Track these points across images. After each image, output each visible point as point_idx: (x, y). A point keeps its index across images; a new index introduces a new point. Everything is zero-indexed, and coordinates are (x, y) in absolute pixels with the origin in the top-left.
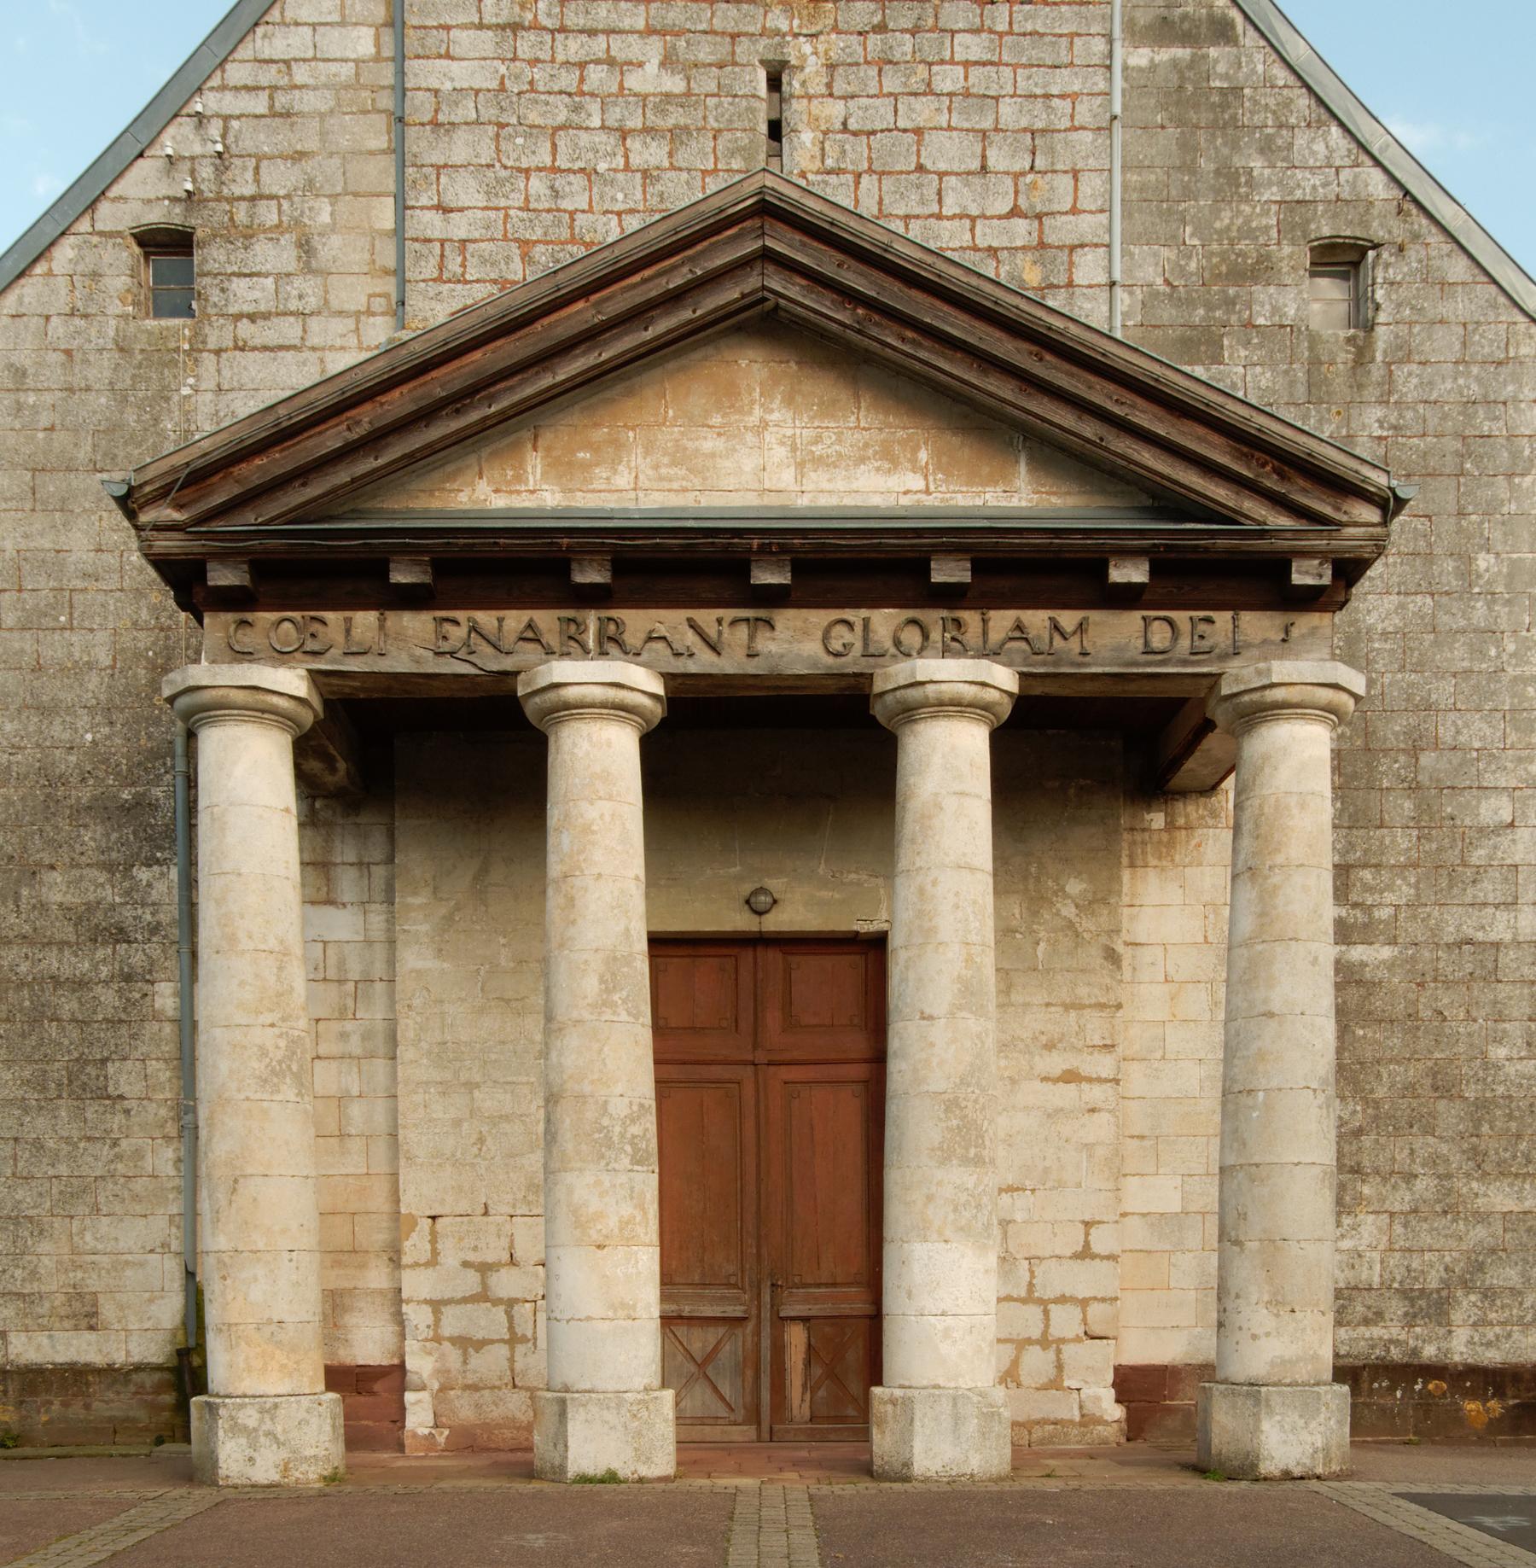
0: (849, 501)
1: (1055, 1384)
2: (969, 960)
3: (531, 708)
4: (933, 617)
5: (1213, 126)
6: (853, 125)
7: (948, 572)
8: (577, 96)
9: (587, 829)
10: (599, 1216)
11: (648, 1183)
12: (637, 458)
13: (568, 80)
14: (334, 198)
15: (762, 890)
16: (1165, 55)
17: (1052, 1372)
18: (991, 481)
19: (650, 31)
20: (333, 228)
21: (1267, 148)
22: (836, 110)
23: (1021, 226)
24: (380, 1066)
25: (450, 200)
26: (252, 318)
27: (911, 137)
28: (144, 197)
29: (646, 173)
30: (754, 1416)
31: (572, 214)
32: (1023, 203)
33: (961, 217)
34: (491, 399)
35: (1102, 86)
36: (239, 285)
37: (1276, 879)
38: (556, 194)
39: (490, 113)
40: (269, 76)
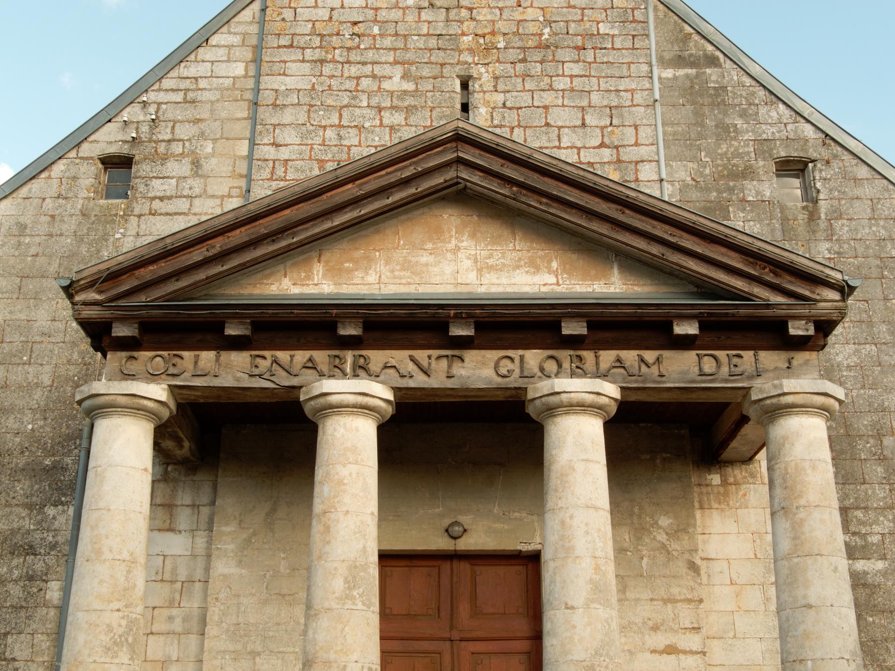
0: (509, 290)
2: (597, 568)
3: (308, 409)
4: (564, 355)
5: (712, 104)
7: (572, 328)
8: (355, 93)
9: (341, 482)
12: (381, 267)
13: (350, 85)
14: (215, 141)
15: (456, 523)
16: (681, 72)
18: (596, 278)
19: (396, 63)
21: (743, 114)
22: (499, 98)
24: (193, 639)
25: (280, 140)
26: (161, 199)
27: (541, 110)
28: (110, 140)
29: (392, 128)
31: (349, 147)
32: (607, 141)
33: (571, 148)
35: (648, 86)
36: (156, 183)
38: (340, 137)
39: (305, 100)
40: (186, 84)
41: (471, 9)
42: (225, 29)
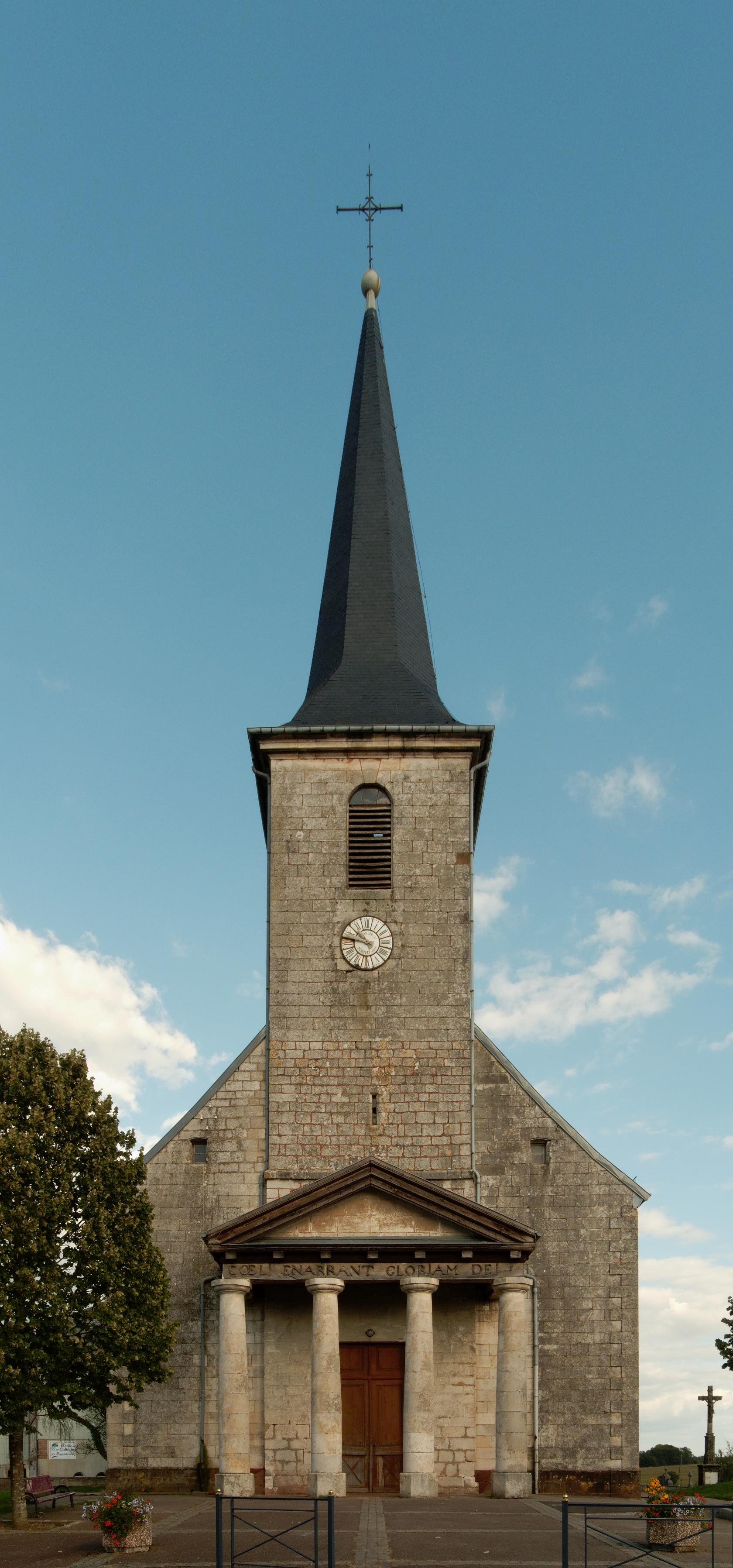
1: (457, 1475)
2: (426, 1356)
3: (309, 1289)
4: (416, 1265)
5: (501, 1106)
6: (397, 1110)
7: (419, 1255)
9: (324, 1322)
10: (326, 1425)
11: (339, 1416)
12: (338, 1224)
13: (316, 1099)
14: (248, 1130)
16: (487, 1086)
17: (456, 1472)
19: (339, 1085)
20: (247, 1138)
21: (517, 1113)
22: (392, 1106)
23: (445, 1138)
25: (282, 1132)
26: (224, 1164)
27: (413, 1114)
28: (194, 1130)
29: (337, 1125)
30: (368, 1485)
32: (446, 1132)
34: (300, 1212)
35: (468, 1099)
36: (220, 1155)
37: (508, 1334)
38: (312, 1131)
39: (293, 1108)
40: (230, 1095)
41: (377, 1050)
42: (247, 1060)
